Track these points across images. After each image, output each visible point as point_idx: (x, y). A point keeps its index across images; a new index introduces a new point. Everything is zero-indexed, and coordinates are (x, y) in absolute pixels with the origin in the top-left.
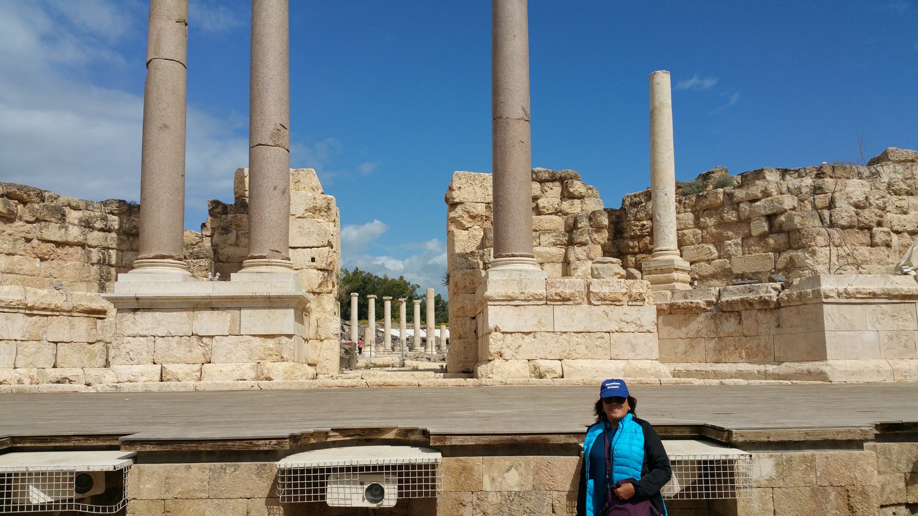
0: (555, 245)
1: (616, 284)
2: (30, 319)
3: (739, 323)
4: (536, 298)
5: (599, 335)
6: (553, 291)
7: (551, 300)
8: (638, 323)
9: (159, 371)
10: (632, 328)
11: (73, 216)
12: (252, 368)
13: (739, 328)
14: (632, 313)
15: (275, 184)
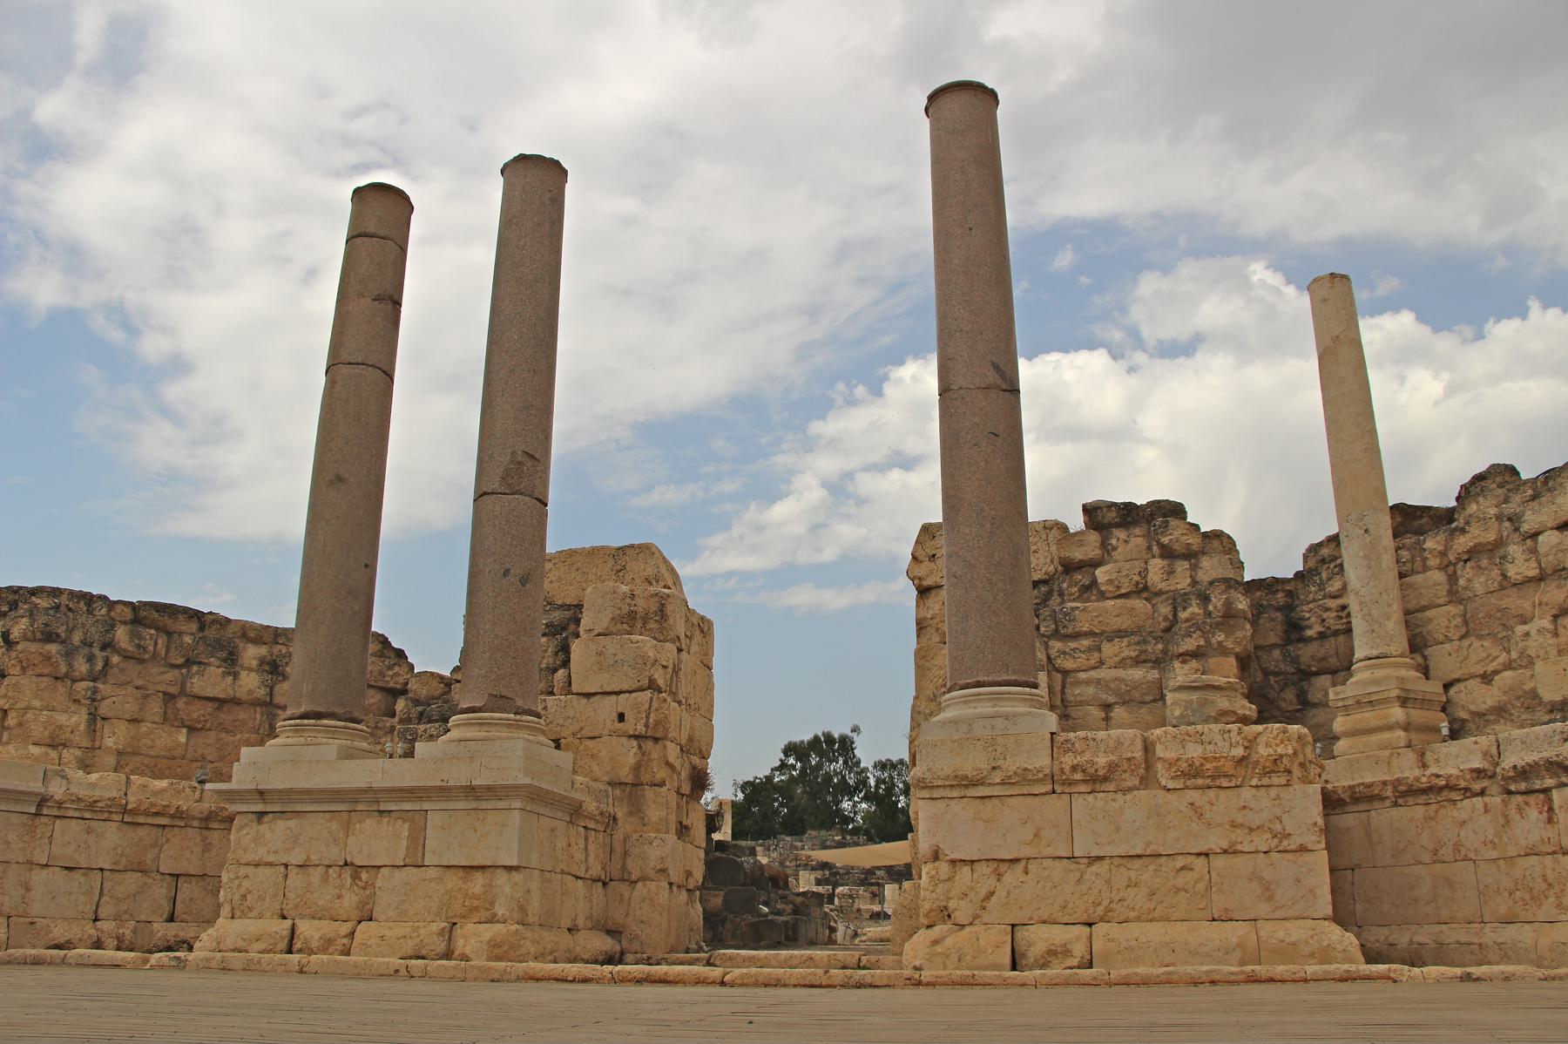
0: (1137, 662)
1: (1218, 738)
2: (130, 832)
3: (1550, 820)
4: (1025, 776)
5: (1180, 862)
6: (1068, 760)
7: (1064, 783)
8: (1278, 827)
9: (286, 933)
10: (1262, 841)
11: (252, 654)
12: (441, 933)
13: (1551, 832)
14: (1257, 802)
15: (507, 566)
